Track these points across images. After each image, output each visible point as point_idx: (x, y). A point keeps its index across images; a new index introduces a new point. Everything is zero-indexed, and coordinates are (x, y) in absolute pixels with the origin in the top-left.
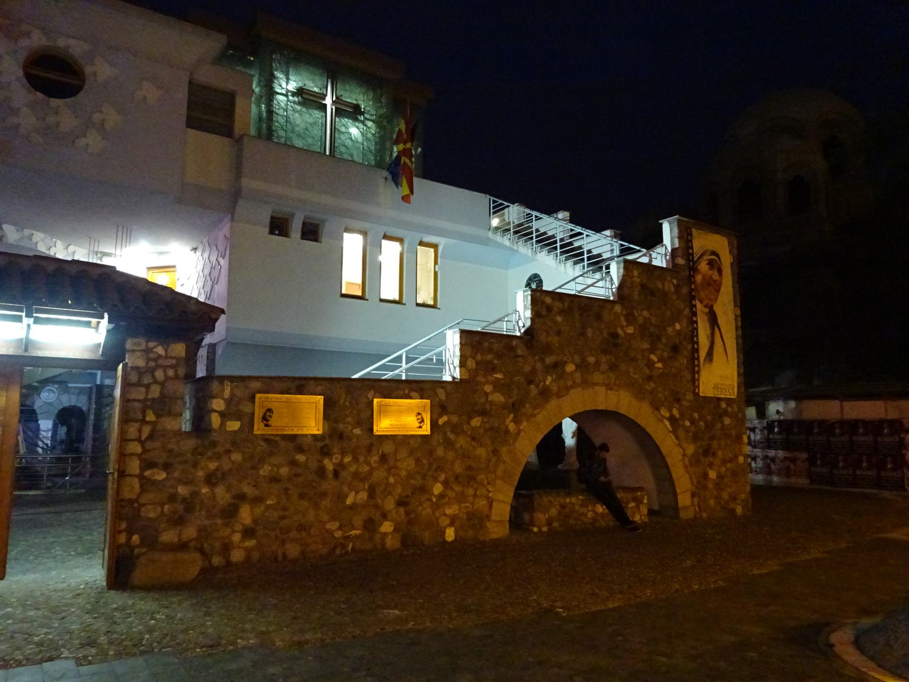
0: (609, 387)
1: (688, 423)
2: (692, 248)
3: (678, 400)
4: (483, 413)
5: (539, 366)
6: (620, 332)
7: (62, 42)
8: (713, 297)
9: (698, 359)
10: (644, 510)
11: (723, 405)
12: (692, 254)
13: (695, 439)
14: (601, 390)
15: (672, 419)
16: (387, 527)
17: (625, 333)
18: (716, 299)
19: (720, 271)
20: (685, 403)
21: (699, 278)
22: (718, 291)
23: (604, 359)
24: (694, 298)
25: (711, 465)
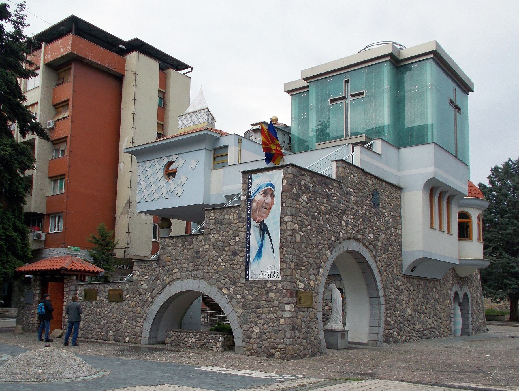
0: (194, 277)
1: (239, 297)
2: (251, 187)
3: (234, 284)
4: (140, 294)
5: (162, 271)
6: (201, 249)
7: (170, 159)
8: (264, 215)
9: (249, 257)
10: (219, 344)
11: (269, 285)
12: (250, 192)
13: (244, 307)
14: (190, 280)
15: (229, 295)
16: (111, 333)
17: (204, 249)
18: (268, 215)
19: (272, 195)
20: (238, 285)
21: (254, 205)
22: (269, 209)
23: (191, 264)
24: (249, 219)
25: (256, 324)
